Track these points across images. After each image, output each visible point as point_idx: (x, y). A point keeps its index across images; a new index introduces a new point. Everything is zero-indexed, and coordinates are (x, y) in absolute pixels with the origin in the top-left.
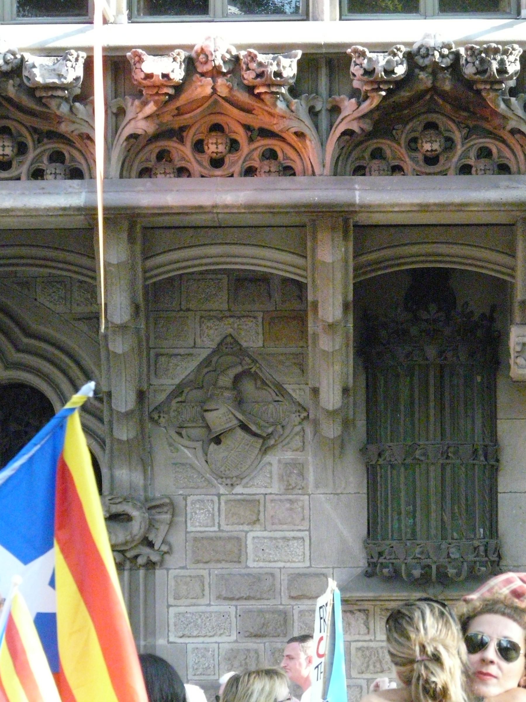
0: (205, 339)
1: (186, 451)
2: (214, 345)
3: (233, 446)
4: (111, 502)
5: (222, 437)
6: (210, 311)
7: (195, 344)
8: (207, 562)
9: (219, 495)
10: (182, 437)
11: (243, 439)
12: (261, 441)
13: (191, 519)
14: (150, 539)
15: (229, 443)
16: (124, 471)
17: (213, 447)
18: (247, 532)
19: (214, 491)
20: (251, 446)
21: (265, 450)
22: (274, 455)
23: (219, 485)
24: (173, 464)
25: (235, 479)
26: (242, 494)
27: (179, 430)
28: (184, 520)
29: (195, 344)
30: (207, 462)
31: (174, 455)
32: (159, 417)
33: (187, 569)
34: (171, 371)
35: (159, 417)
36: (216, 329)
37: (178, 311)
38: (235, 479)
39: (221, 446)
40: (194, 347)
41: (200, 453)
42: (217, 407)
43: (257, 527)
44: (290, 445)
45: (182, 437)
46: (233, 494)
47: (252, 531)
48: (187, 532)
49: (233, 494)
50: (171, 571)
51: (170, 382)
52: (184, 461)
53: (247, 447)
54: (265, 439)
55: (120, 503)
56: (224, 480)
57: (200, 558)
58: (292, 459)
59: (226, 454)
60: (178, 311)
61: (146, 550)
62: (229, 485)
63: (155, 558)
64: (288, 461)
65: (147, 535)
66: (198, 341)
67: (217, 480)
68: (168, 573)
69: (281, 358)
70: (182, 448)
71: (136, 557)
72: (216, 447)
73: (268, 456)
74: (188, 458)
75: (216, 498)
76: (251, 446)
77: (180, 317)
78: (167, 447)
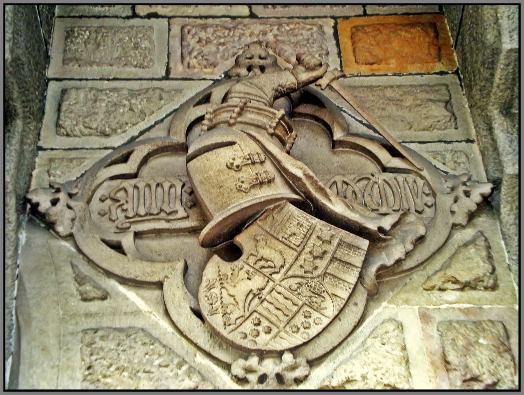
0: (194, 62)
1: (131, 295)
2: (218, 74)
3: (278, 262)
5: (242, 239)
6: (206, 17)
7: (168, 71)
10: (124, 253)
11: (307, 237)
12: (364, 243)
17: (216, 266)
20: (334, 259)
21: (379, 284)
22: (407, 302)
24: (85, 331)
25: (288, 357)
27: (114, 238)
29: (168, 71)
30: (198, 314)
31: (94, 306)
32: (54, 202)
34: (101, 116)
35: (54, 202)
36: (223, 44)
37: (128, 18)
38: (288, 357)
39: (239, 263)
40: (167, 77)
41: (175, 292)
42: (229, 139)
44: (450, 273)
45: (124, 253)
51: (97, 141)
52: (124, 322)
53: (322, 264)
54: (377, 239)
56: (253, 361)
58: (466, 312)
59: (258, 281)
60: (128, 18)
64: (453, 316)
66: (178, 69)
67: (227, 367)
69: (389, 93)
70: (122, 289)
72: (226, 267)
73: (384, 304)
74: (137, 312)
76: (334, 259)
77: (132, 27)
78: (73, 287)
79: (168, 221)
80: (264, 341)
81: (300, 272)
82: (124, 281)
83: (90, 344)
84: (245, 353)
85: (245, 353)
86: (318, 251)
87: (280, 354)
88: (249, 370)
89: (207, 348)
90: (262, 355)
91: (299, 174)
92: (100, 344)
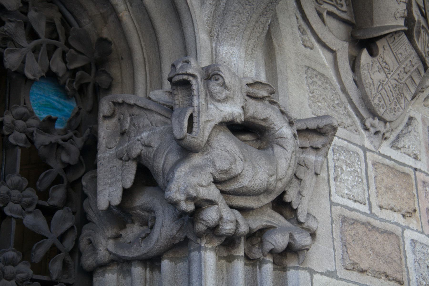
4: (251, 90)
8: (363, 271)
9: (365, 150)
11: (406, 59)
13: (335, 179)
14: (288, 198)
15: (387, 59)
16: (235, 50)
18: (404, 228)
19: (356, 138)
23: (363, 131)
24: (309, 68)
26: (389, 158)
28: (326, 178)
33: (338, 278)
39: (375, 59)
43: (413, 223)
46: (380, 154)
47: (408, 228)
48: (332, 204)
49: (380, 154)
50: (316, 277)
53: (406, 76)
55: (262, 99)
57: (356, 259)
61: (277, 219)
62: (380, 135)
63: (302, 239)
65: (286, 189)
68: (312, 278)
71: (262, 231)
74: (323, 65)
75: (361, 153)
78: (298, 33)
79: (338, 9)
80: (381, 111)
81: (397, 78)
82: (319, 40)
83: (311, 77)
84: (374, 114)
85: (374, 114)
86: (407, 69)
87: (385, 122)
88: (372, 126)
89: (356, 104)
90: (381, 119)
91: (416, 18)
92: (315, 79)
